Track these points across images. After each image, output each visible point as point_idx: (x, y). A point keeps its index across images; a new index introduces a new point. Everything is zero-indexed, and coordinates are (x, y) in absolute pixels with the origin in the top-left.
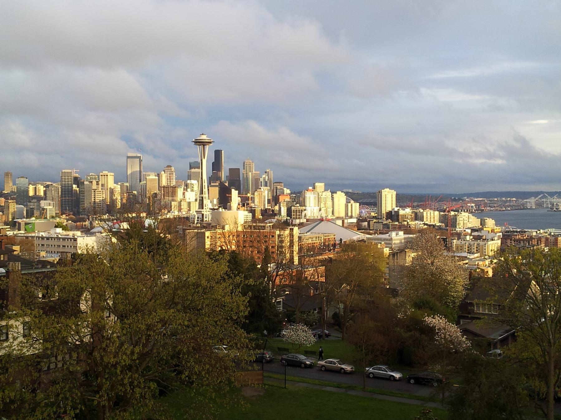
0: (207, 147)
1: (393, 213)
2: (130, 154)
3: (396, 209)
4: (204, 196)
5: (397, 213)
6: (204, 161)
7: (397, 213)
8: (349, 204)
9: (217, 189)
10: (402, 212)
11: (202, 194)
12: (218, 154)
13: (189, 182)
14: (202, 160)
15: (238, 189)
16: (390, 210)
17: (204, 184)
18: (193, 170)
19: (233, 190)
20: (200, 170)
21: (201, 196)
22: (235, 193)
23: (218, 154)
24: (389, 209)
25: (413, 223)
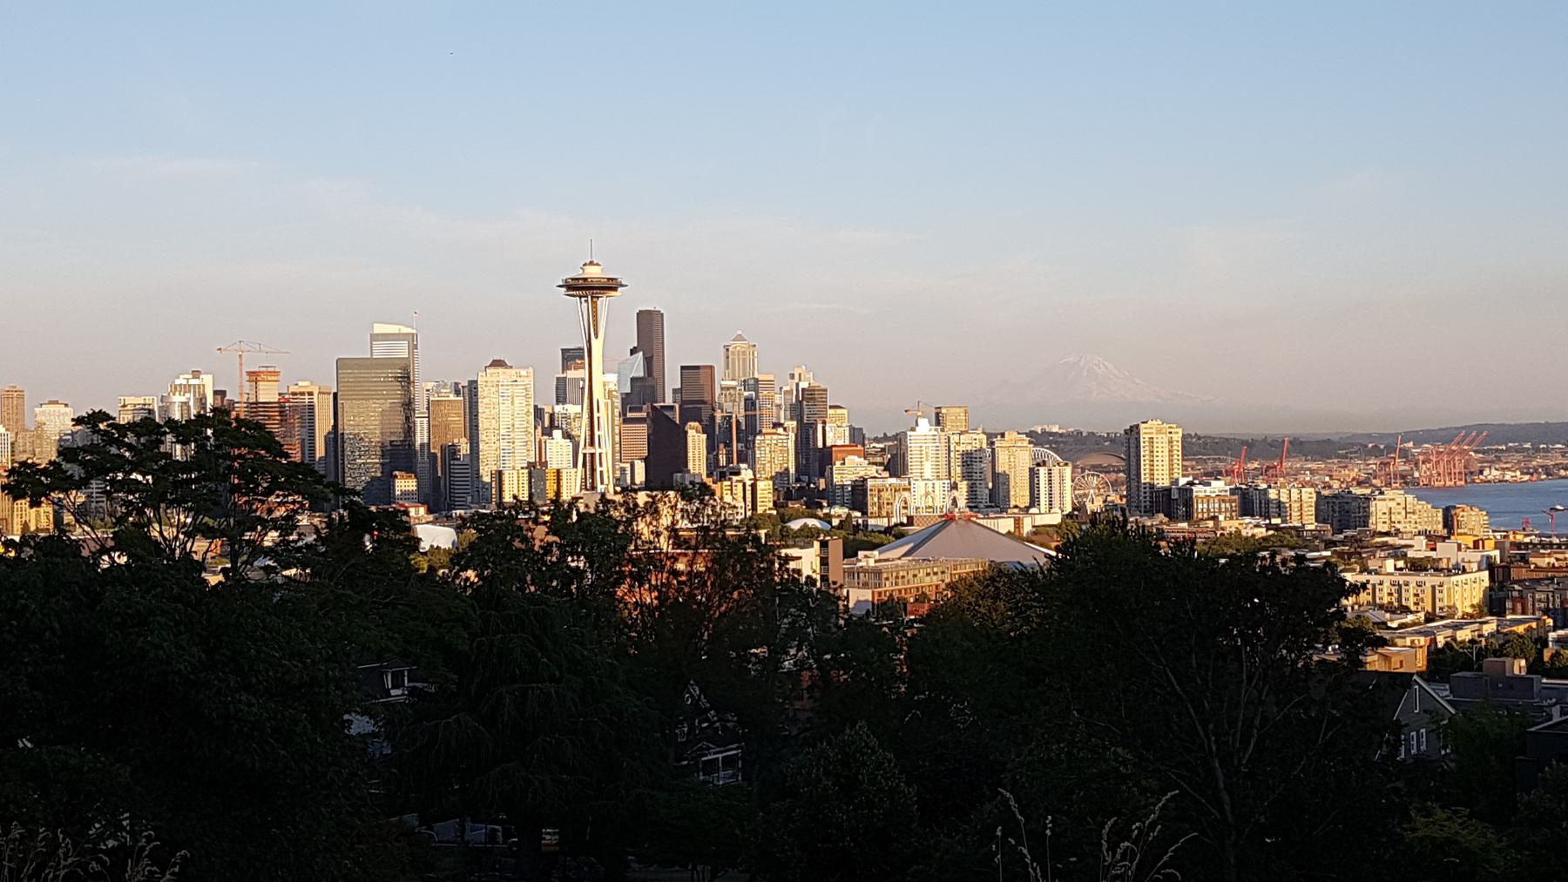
0: (603, 302)
1: (1175, 495)
2: (379, 329)
3: (1183, 481)
4: (598, 451)
5: (1186, 492)
6: (597, 345)
7: (1186, 492)
8: (1043, 471)
9: (643, 429)
10: (1198, 490)
11: (592, 444)
12: (649, 323)
13: (558, 408)
14: (589, 342)
15: (708, 429)
16: (1167, 483)
17: (596, 415)
18: (571, 374)
19: (691, 433)
20: (584, 373)
21: (589, 450)
22: (696, 441)
23: (649, 323)
24: (1162, 481)
25: (1235, 523)
